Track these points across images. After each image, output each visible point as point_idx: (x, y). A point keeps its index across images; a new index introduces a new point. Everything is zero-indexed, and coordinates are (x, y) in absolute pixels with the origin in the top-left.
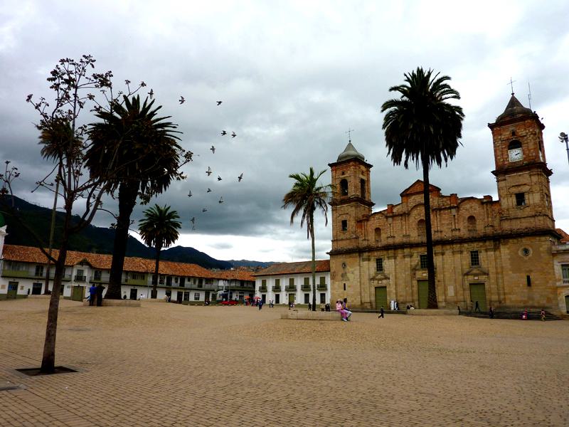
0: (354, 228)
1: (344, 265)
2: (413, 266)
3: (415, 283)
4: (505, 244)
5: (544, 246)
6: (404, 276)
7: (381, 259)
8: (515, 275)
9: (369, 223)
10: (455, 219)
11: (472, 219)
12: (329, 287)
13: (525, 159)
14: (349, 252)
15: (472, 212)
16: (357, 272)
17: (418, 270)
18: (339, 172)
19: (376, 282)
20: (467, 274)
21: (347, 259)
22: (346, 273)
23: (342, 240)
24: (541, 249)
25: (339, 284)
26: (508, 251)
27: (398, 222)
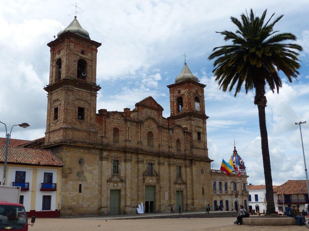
0: (93, 120)
1: (81, 162)
3: (145, 186)
4: (195, 165)
6: (136, 180)
7: (118, 161)
9: (108, 121)
10: (171, 140)
11: (178, 141)
12: (58, 187)
13: (201, 111)
16: (96, 172)
17: (147, 175)
19: (112, 184)
20: (175, 183)
21: (87, 156)
22: (83, 172)
23: (78, 130)
25: (72, 184)
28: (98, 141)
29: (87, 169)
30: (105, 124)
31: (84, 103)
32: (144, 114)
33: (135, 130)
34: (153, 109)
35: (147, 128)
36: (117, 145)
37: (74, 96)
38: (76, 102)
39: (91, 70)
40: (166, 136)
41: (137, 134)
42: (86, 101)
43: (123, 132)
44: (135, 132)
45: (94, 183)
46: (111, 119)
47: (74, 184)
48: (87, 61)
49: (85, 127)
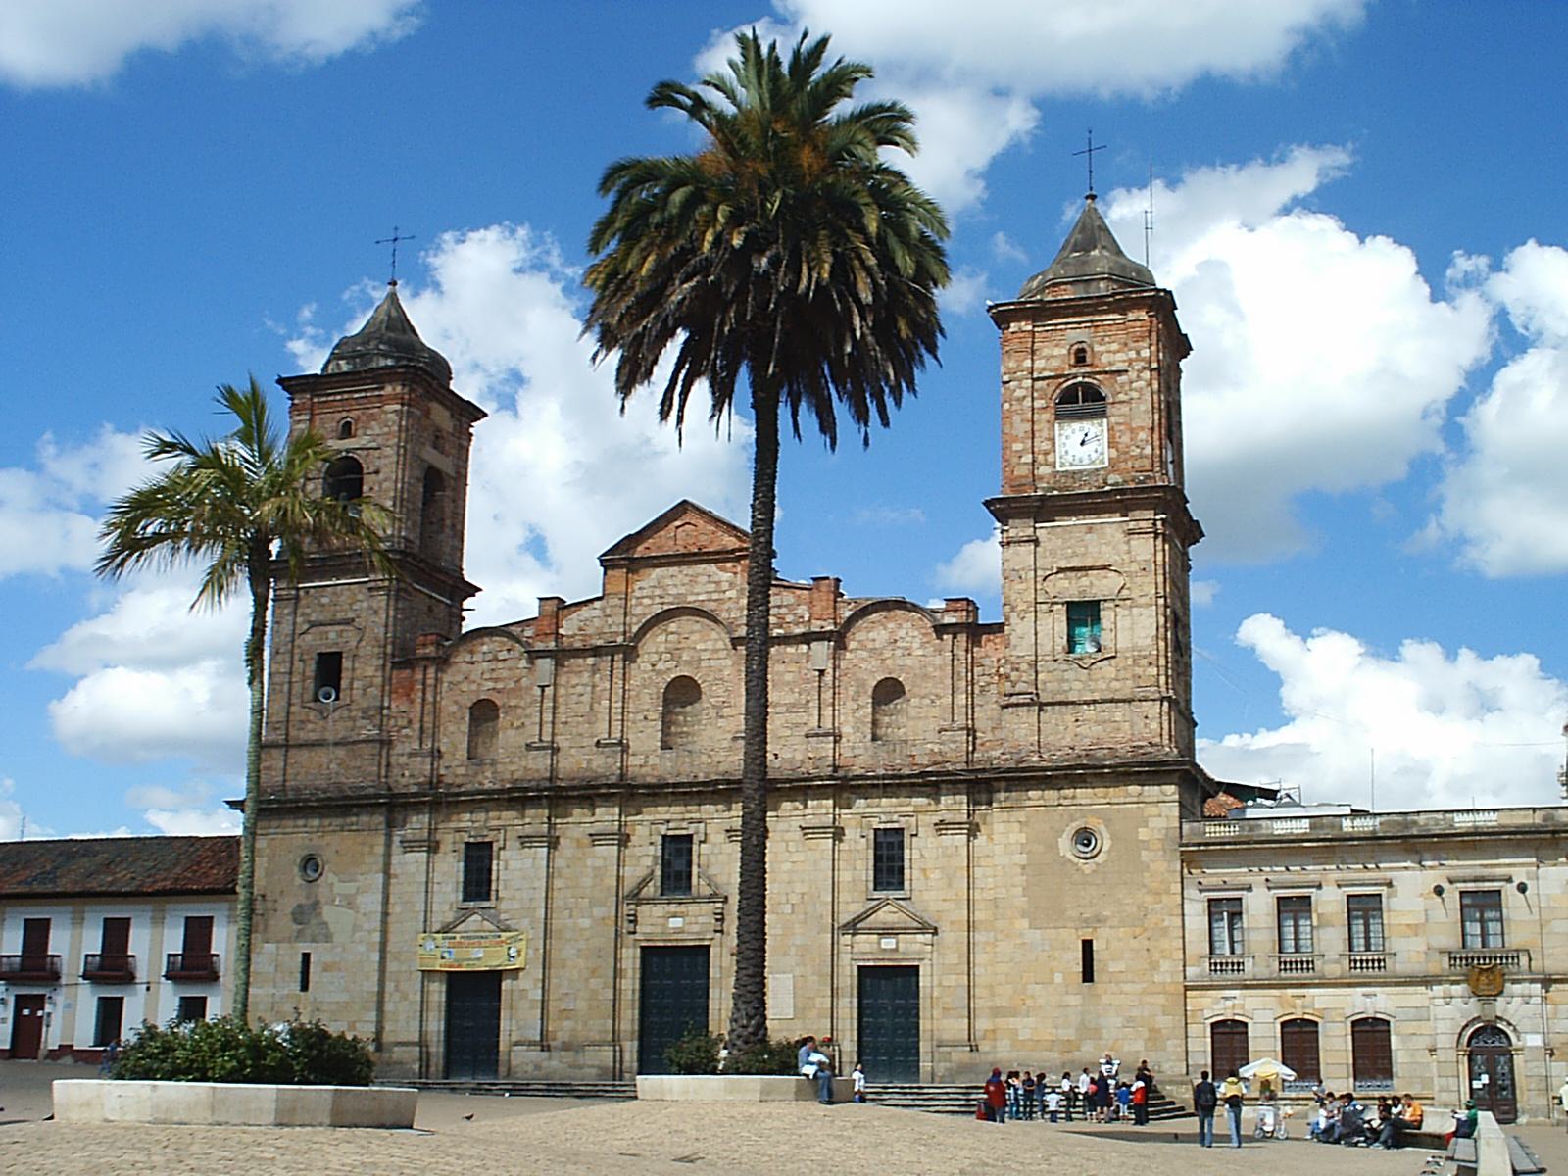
0: (374, 691)
1: (310, 864)
2: (629, 884)
5: (1154, 823)
8: (1036, 935)
14: (339, 805)
15: (895, 666)
16: (372, 902)
17: (649, 901)
18: (327, 424)
20: (853, 927)
22: (316, 905)
24: (1143, 834)
26: (1022, 838)
27: (581, 679)
28: (396, 771)
29: (336, 891)
30: (424, 693)
31: (340, 634)
32: (646, 601)
33: (589, 689)
34: (701, 562)
35: (660, 666)
36: (488, 774)
37: (303, 615)
38: (308, 637)
39: (376, 488)
40: (788, 677)
41: (596, 705)
42: (349, 622)
43: (520, 711)
44: (586, 698)
45: (362, 948)
46: (464, 667)
47: (281, 952)
48: (359, 456)
49: (340, 725)
